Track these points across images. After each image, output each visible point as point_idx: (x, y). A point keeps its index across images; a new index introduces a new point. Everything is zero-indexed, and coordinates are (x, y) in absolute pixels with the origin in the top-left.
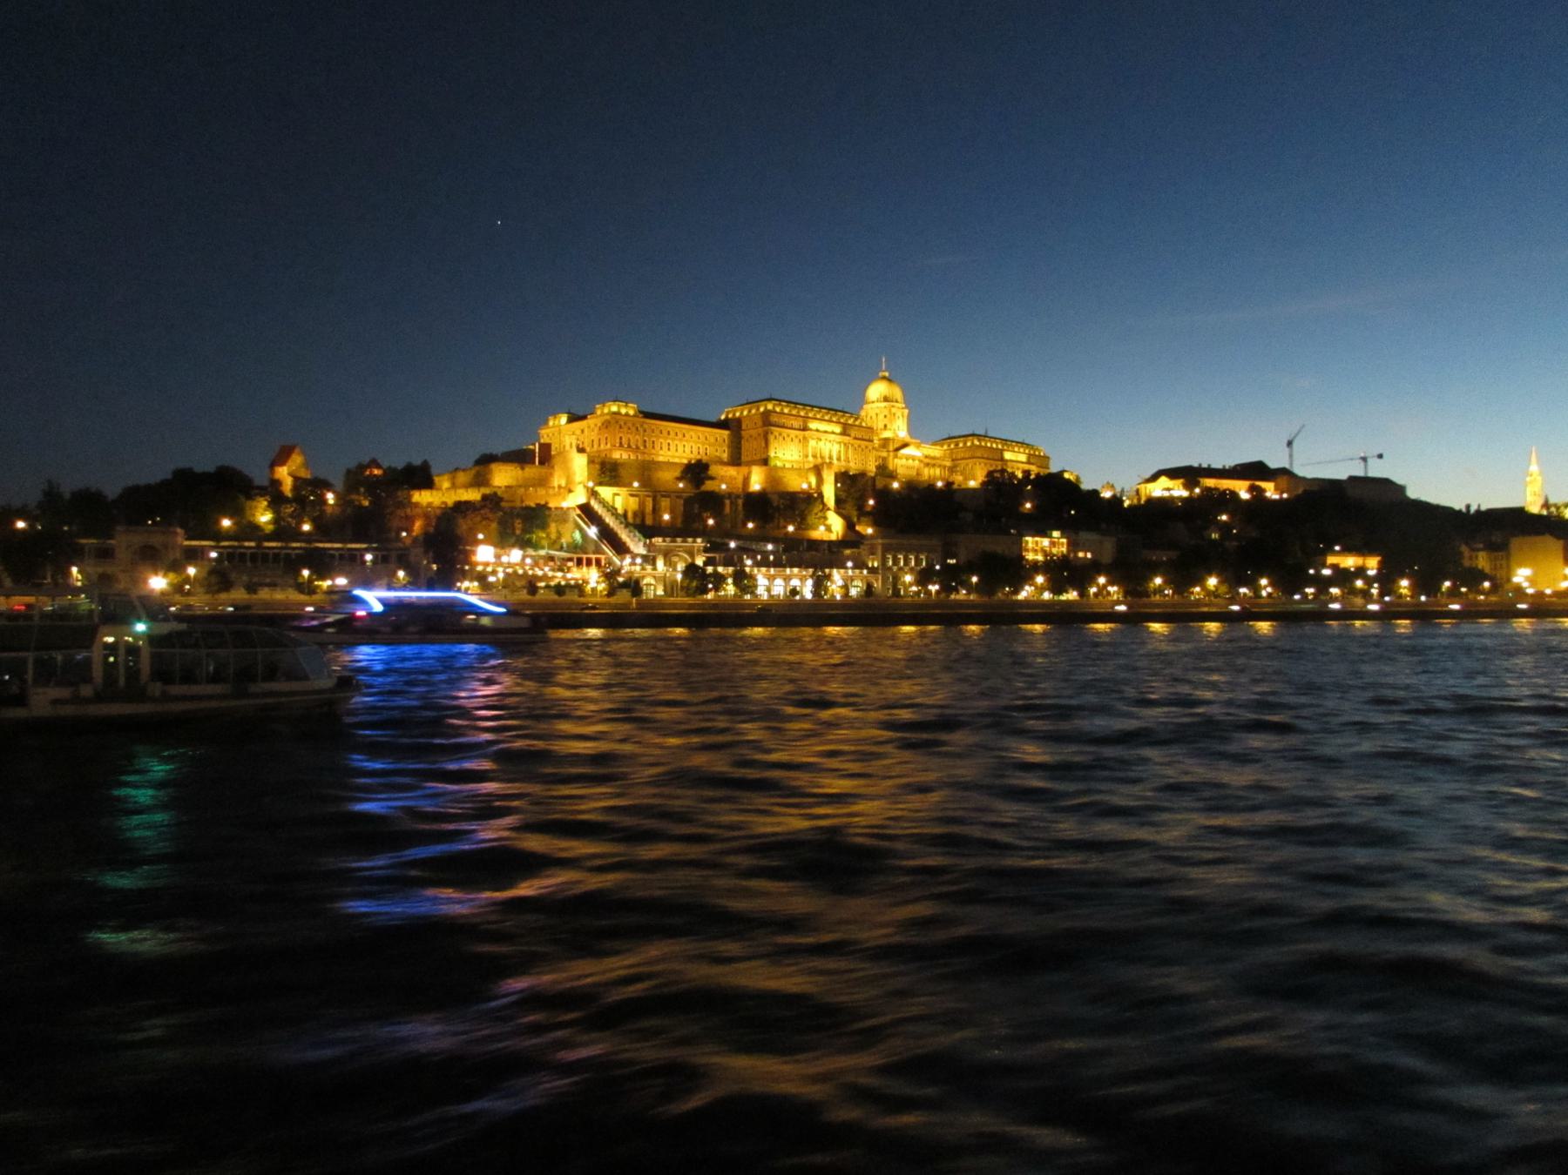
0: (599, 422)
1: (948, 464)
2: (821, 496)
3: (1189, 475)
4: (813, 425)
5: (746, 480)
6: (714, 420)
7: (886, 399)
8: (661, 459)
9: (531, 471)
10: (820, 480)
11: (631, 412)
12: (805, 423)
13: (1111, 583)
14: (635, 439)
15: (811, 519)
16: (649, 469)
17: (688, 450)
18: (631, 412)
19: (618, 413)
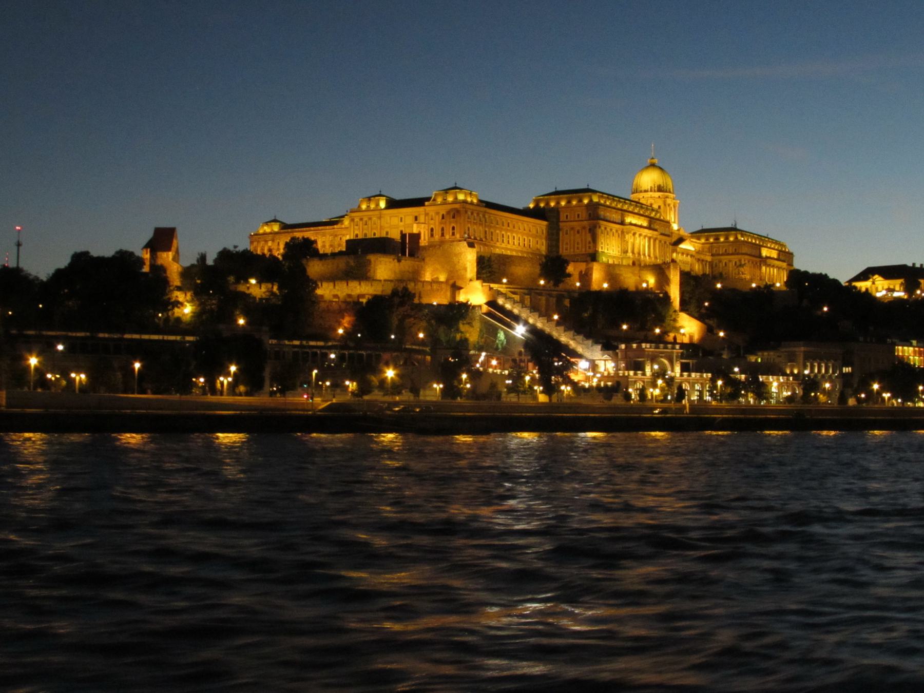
0: (443, 210)
1: (709, 258)
2: (667, 298)
3: (909, 275)
4: (629, 219)
5: (585, 277)
6: (520, 207)
7: (660, 189)
8: (498, 251)
9: (407, 264)
10: (663, 279)
11: (475, 201)
12: (623, 217)
13: (883, 389)
14: (478, 231)
15: (668, 320)
16: (504, 264)
17: (516, 242)
18: (475, 201)
19: (465, 202)
